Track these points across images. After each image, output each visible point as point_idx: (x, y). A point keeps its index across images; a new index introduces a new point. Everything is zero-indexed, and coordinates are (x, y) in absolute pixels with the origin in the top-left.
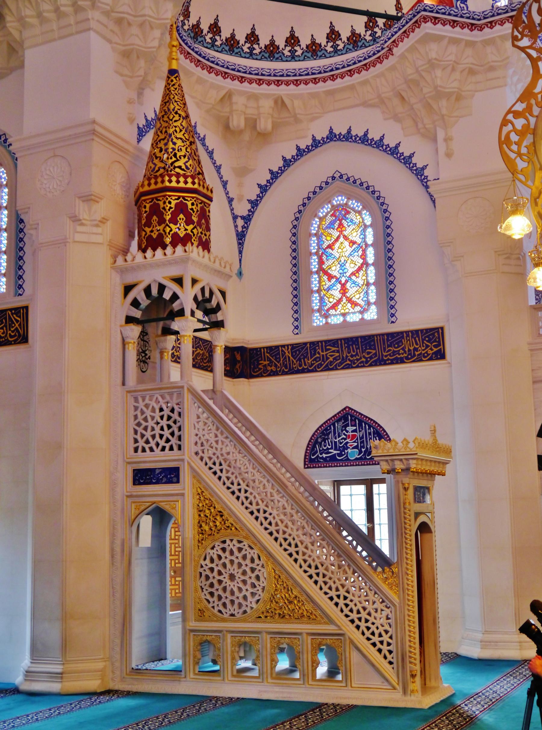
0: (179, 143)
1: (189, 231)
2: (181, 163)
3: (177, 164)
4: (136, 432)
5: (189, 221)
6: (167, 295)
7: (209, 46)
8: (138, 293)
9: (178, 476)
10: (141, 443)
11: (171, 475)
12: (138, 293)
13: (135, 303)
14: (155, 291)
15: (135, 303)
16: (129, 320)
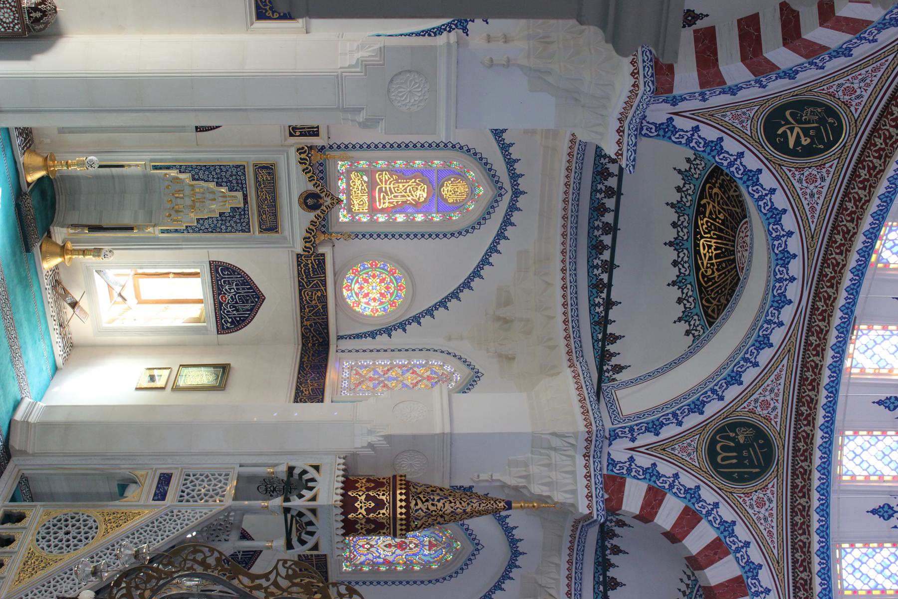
0: (440, 505)
1: (360, 511)
2: (420, 505)
3: (419, 501)
4: (201, 475)
5: (368, 511)
6: (304, 492)
7: (596, 579)
8: (312, 473)
9: (158, 500)
10: (192, 478)
11: (161, 495)
12: (312, 473)
13: (305, 472)
14: (310, 484)
15: (305, 472)
16: (291, 469)
